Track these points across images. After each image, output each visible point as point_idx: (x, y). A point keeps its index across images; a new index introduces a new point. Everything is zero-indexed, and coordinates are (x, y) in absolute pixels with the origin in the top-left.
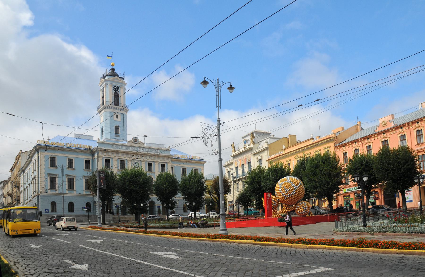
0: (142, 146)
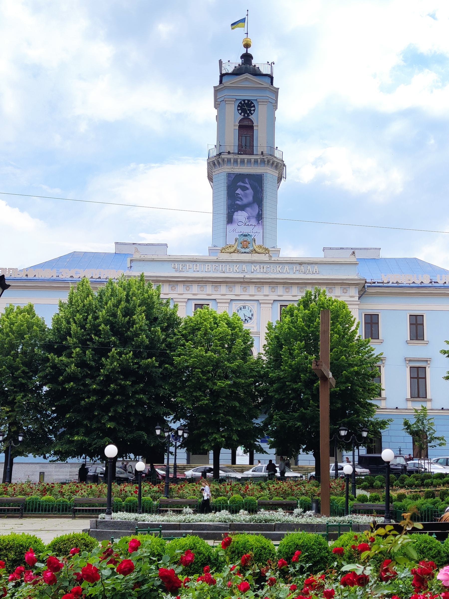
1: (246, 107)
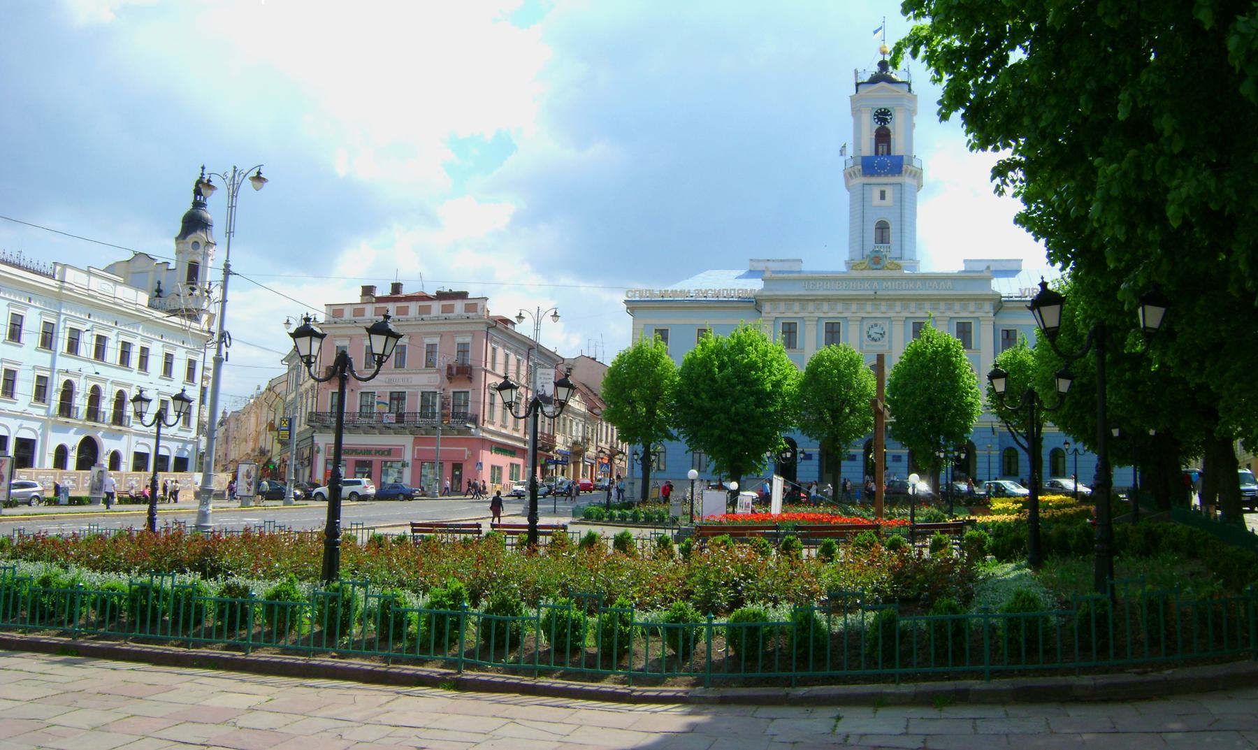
0: (895, 273)
1: (882, 116)
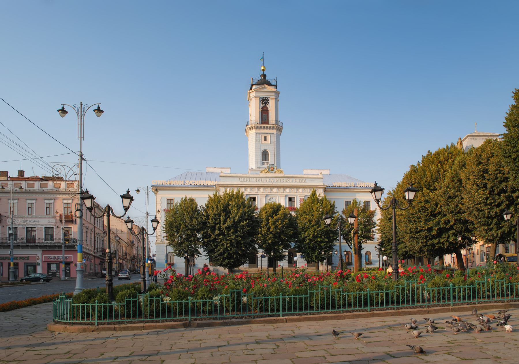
1: (265, 101)
